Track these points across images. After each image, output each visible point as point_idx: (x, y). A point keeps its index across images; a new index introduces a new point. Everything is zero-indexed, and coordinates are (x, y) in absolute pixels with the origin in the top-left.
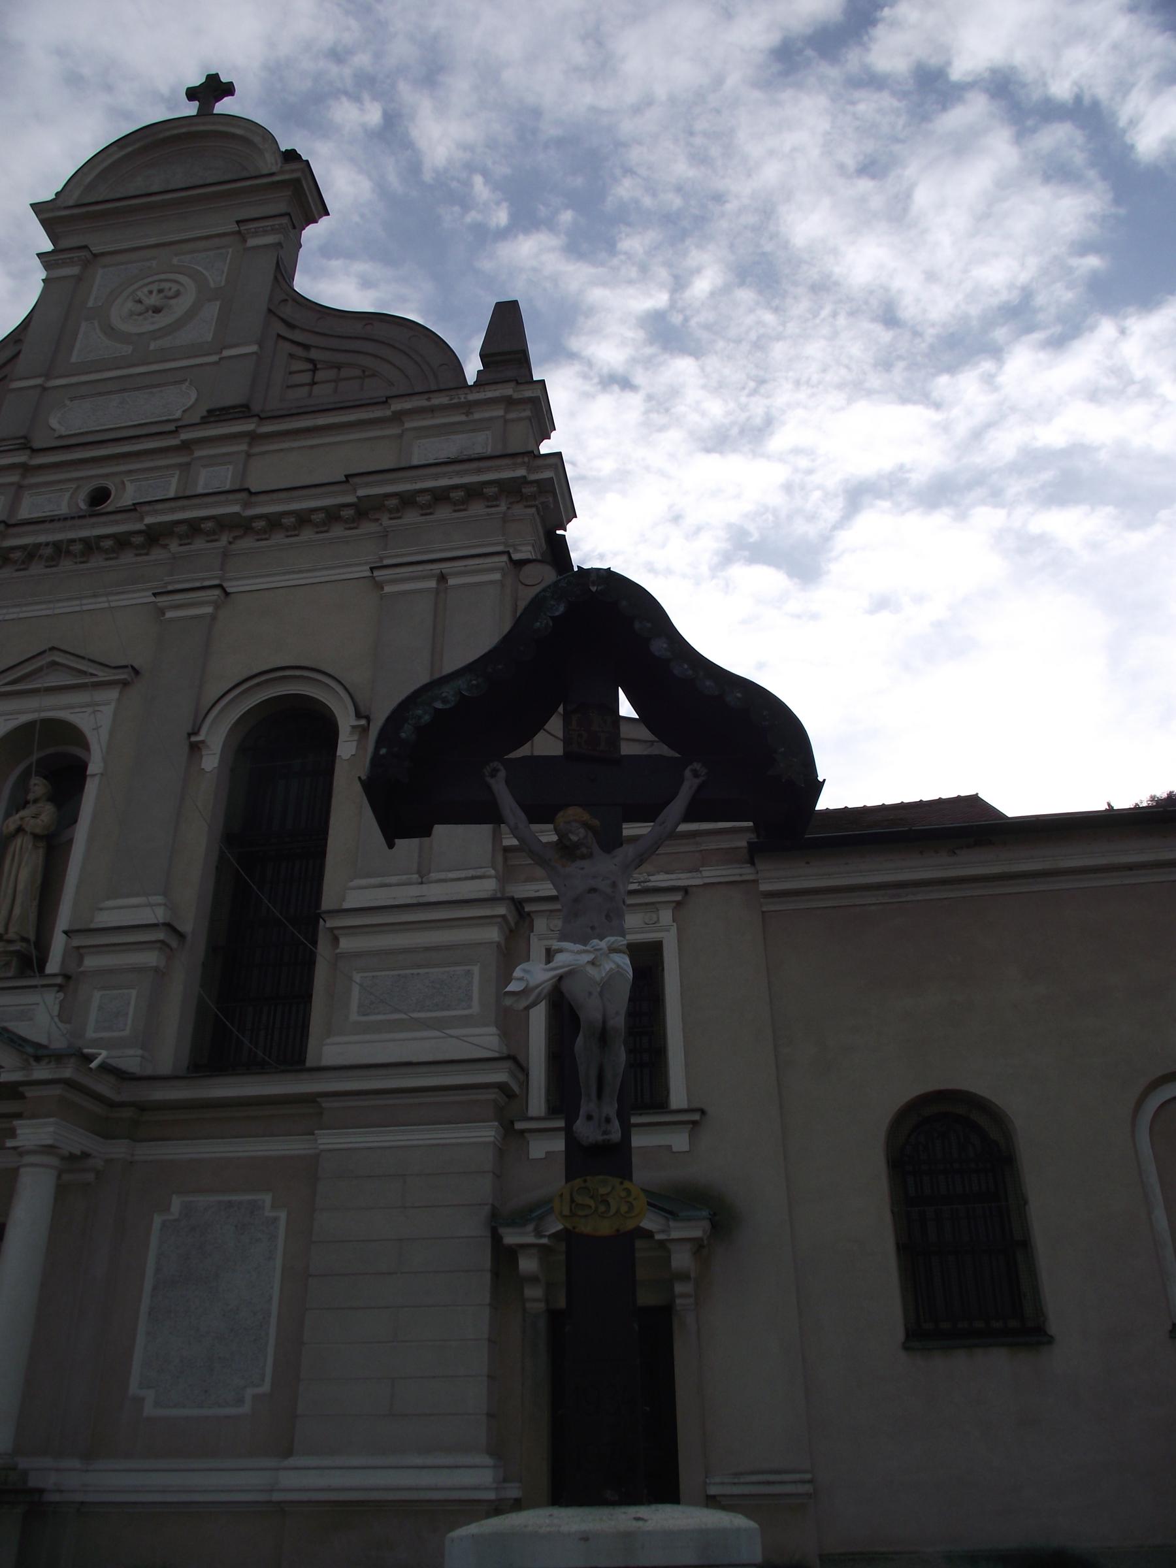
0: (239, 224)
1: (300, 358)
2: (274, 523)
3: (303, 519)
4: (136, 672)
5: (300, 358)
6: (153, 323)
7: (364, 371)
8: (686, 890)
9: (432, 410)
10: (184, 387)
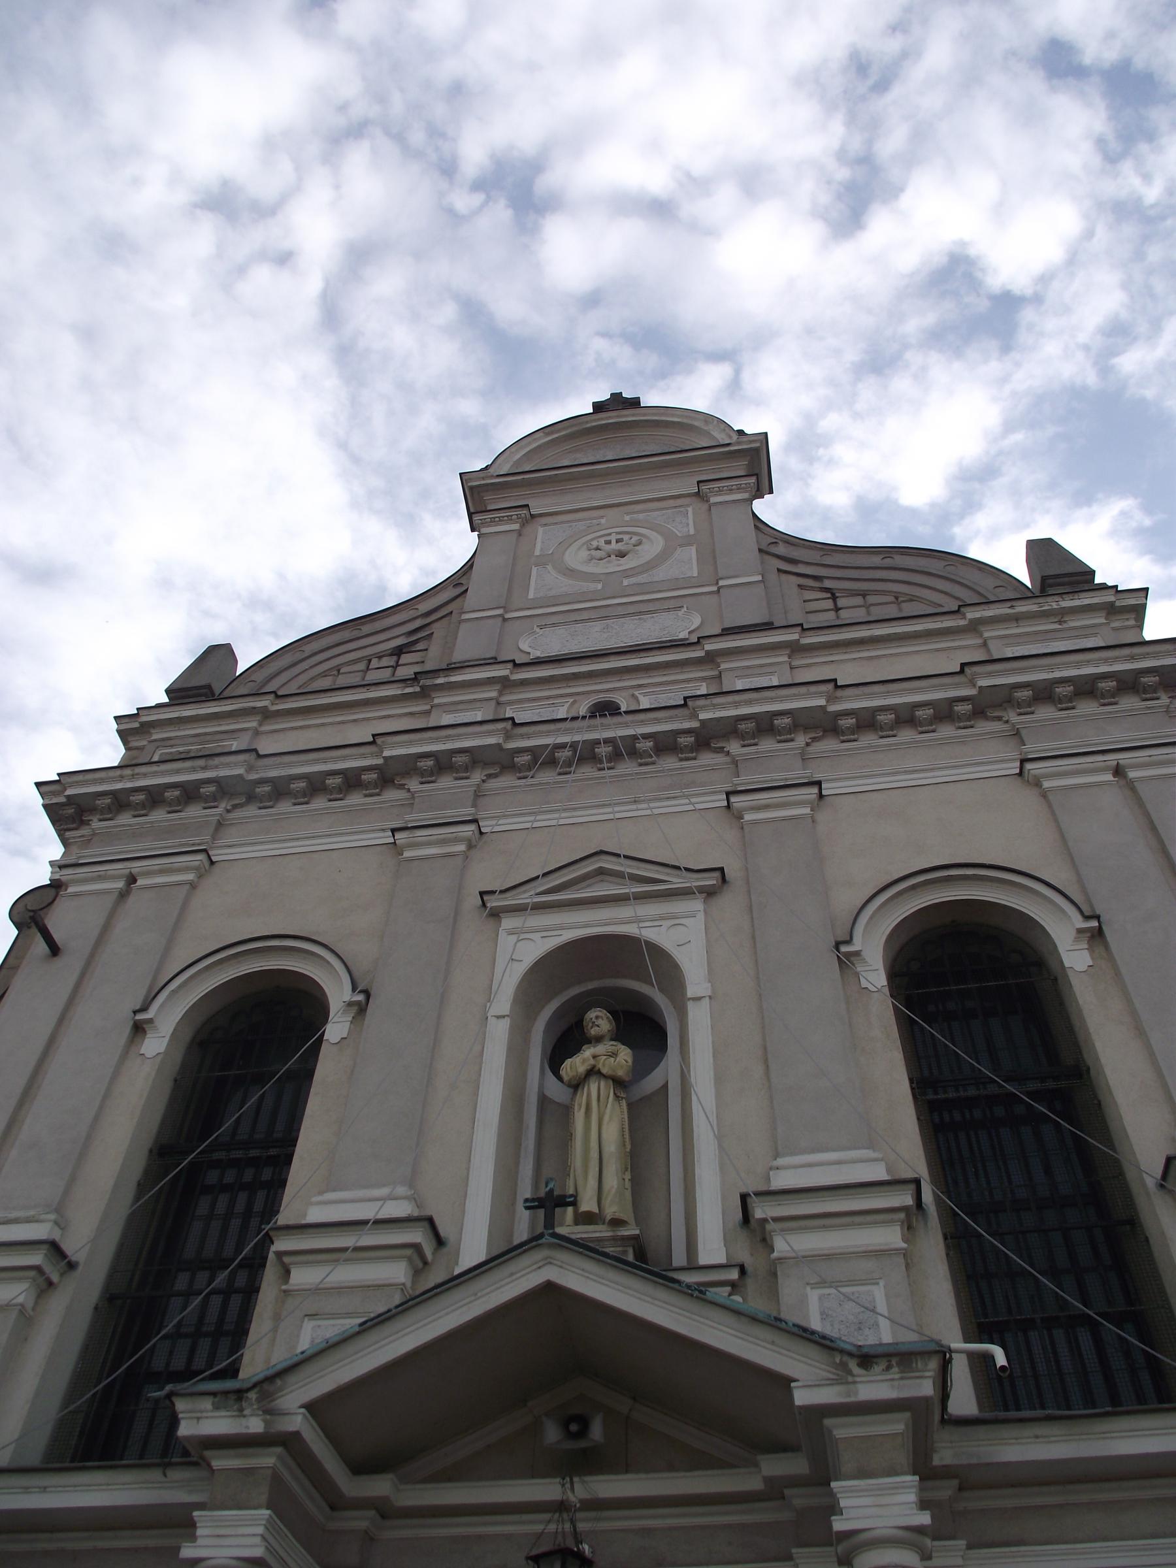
0: (701, 485)
1: (812, 588)
2: (867, 722)
3: (906, 718)
6: (619, 565)
7: (897, 598)
9: (1017, 619)
10: (680, 613)
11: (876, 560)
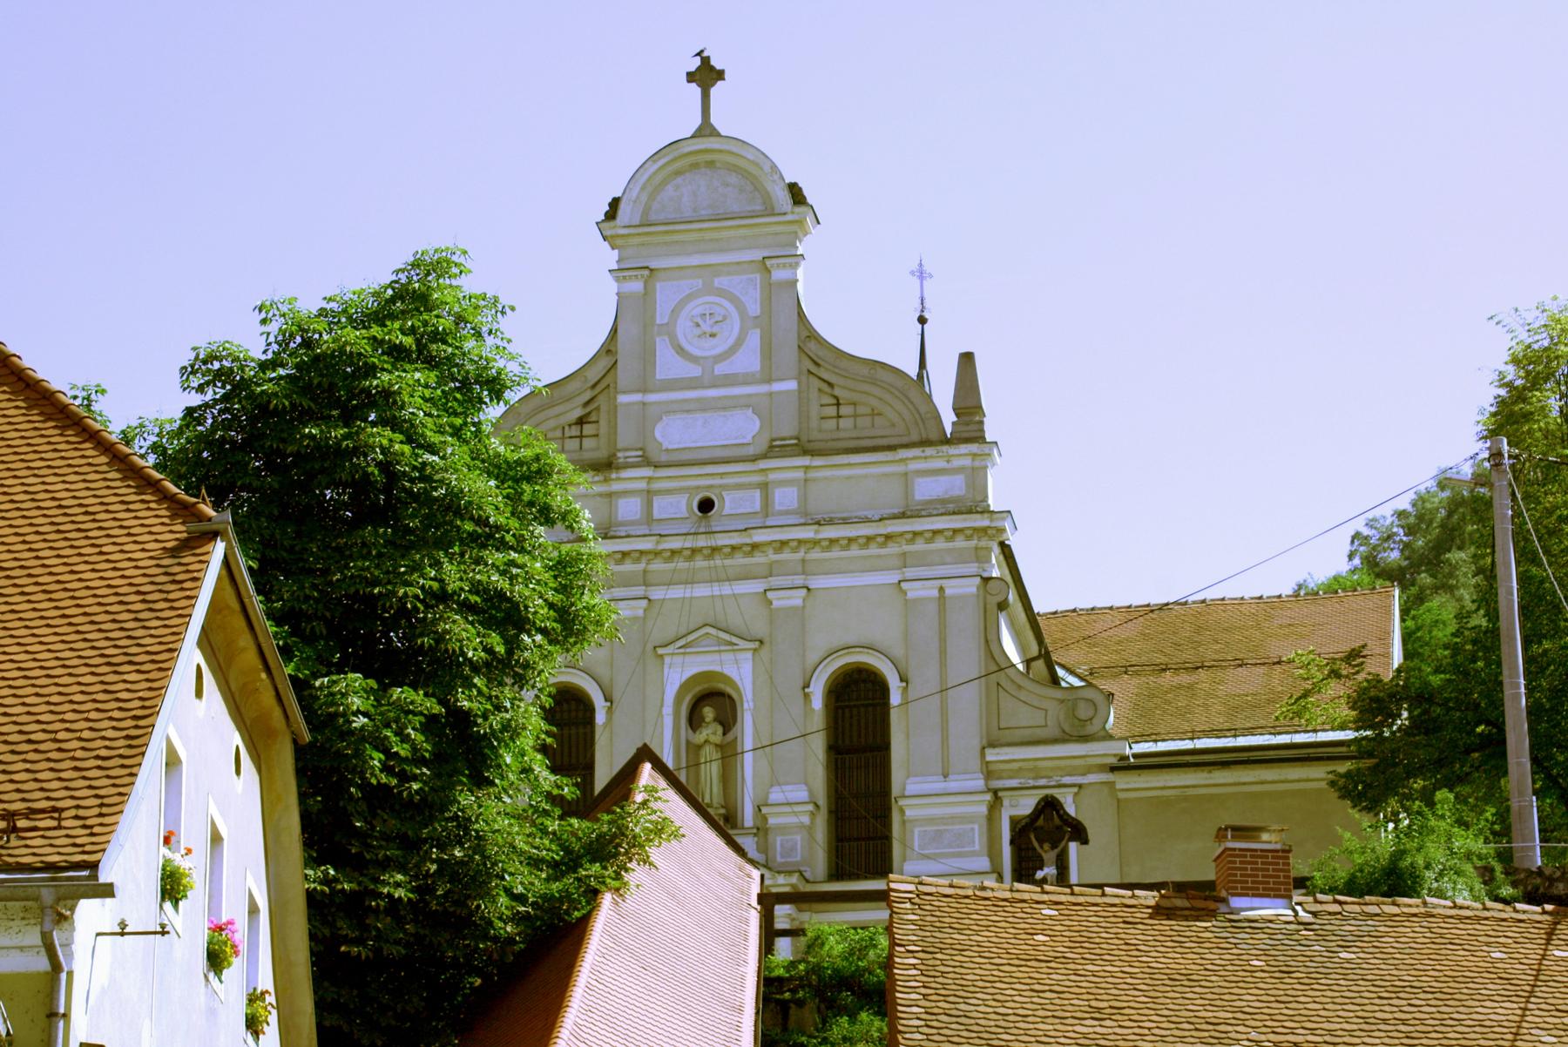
1: (826, 393)
4: (761, 642)
5: (826, 393)
7: (873, 410)
8: (1080, 786)
11: (865, 371)
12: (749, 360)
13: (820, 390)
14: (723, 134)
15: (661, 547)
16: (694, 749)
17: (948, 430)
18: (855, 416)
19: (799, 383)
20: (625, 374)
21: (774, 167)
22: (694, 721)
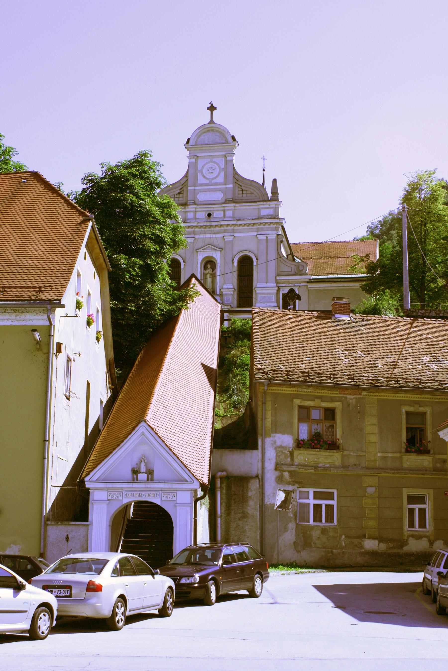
4: (222, 249)
8: (299, 286)
11: (249, 183)
12: (221, 179)
13: (238, 187)
14: (216, 122)
15: (198, 225)
16: (205, 275)
17: (270, 198)
18: (247, 194)
19: (233, 185)
20: (190, 182)
21: (228, 132)
22: (205, 268)
